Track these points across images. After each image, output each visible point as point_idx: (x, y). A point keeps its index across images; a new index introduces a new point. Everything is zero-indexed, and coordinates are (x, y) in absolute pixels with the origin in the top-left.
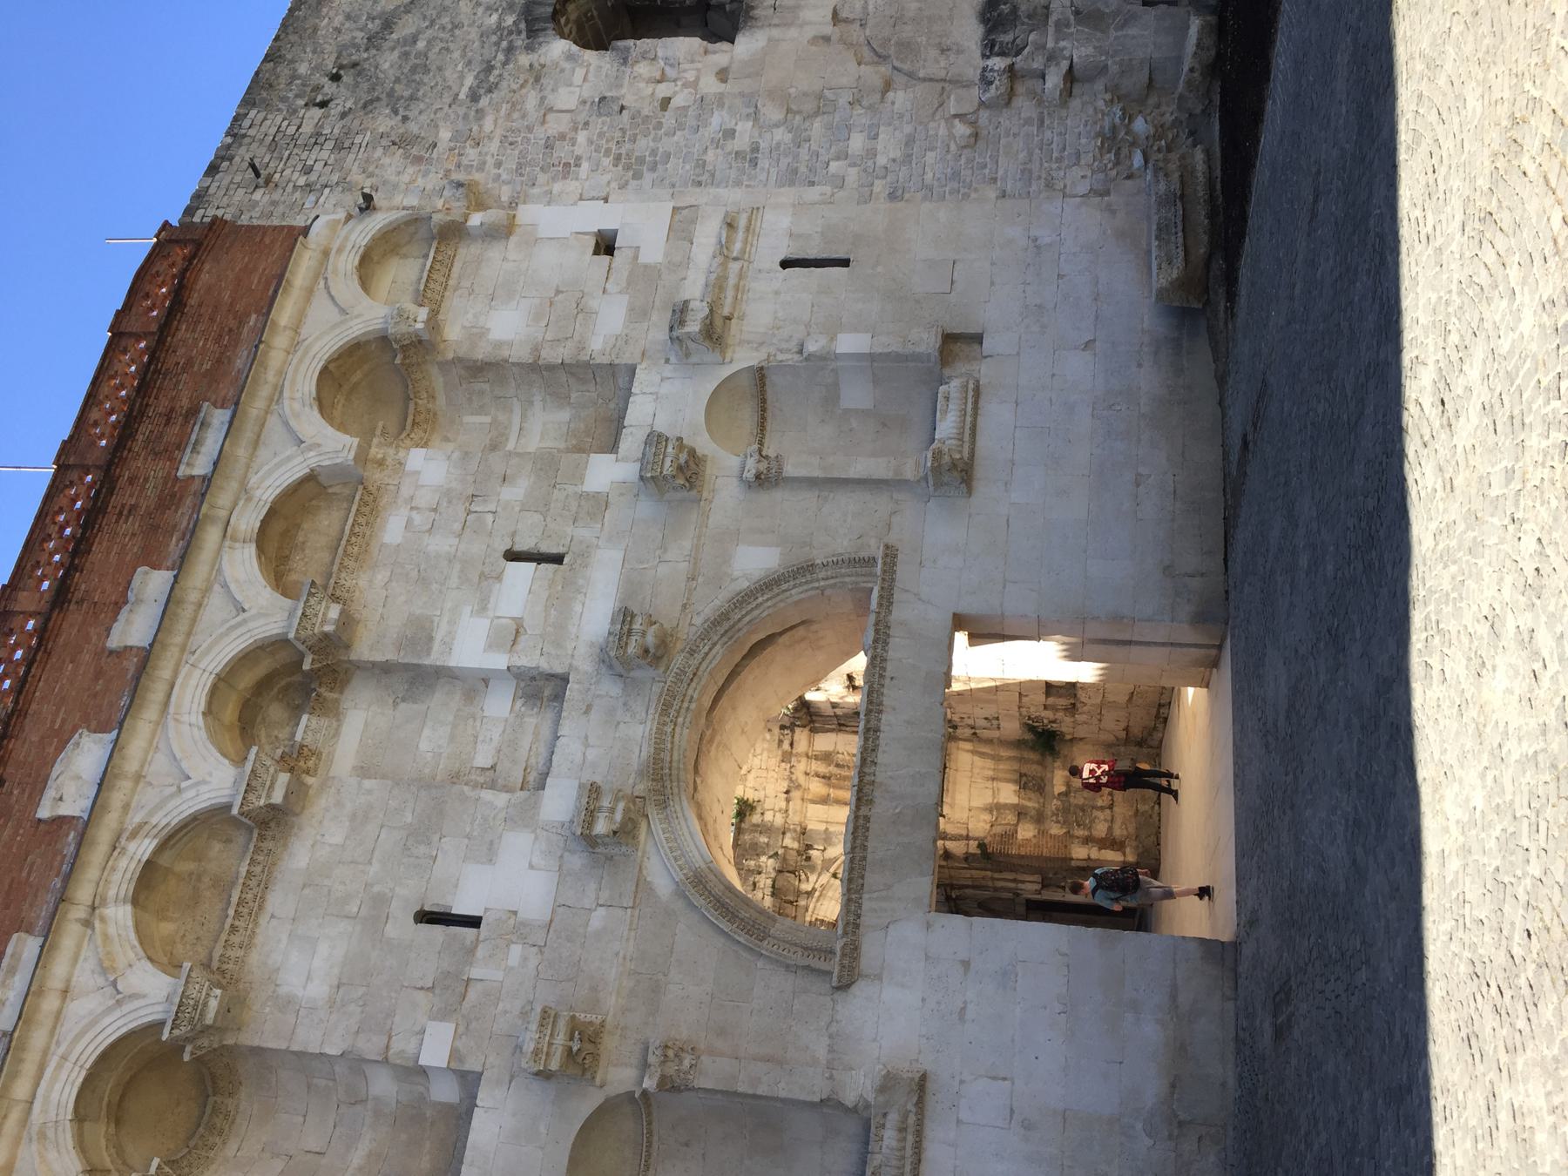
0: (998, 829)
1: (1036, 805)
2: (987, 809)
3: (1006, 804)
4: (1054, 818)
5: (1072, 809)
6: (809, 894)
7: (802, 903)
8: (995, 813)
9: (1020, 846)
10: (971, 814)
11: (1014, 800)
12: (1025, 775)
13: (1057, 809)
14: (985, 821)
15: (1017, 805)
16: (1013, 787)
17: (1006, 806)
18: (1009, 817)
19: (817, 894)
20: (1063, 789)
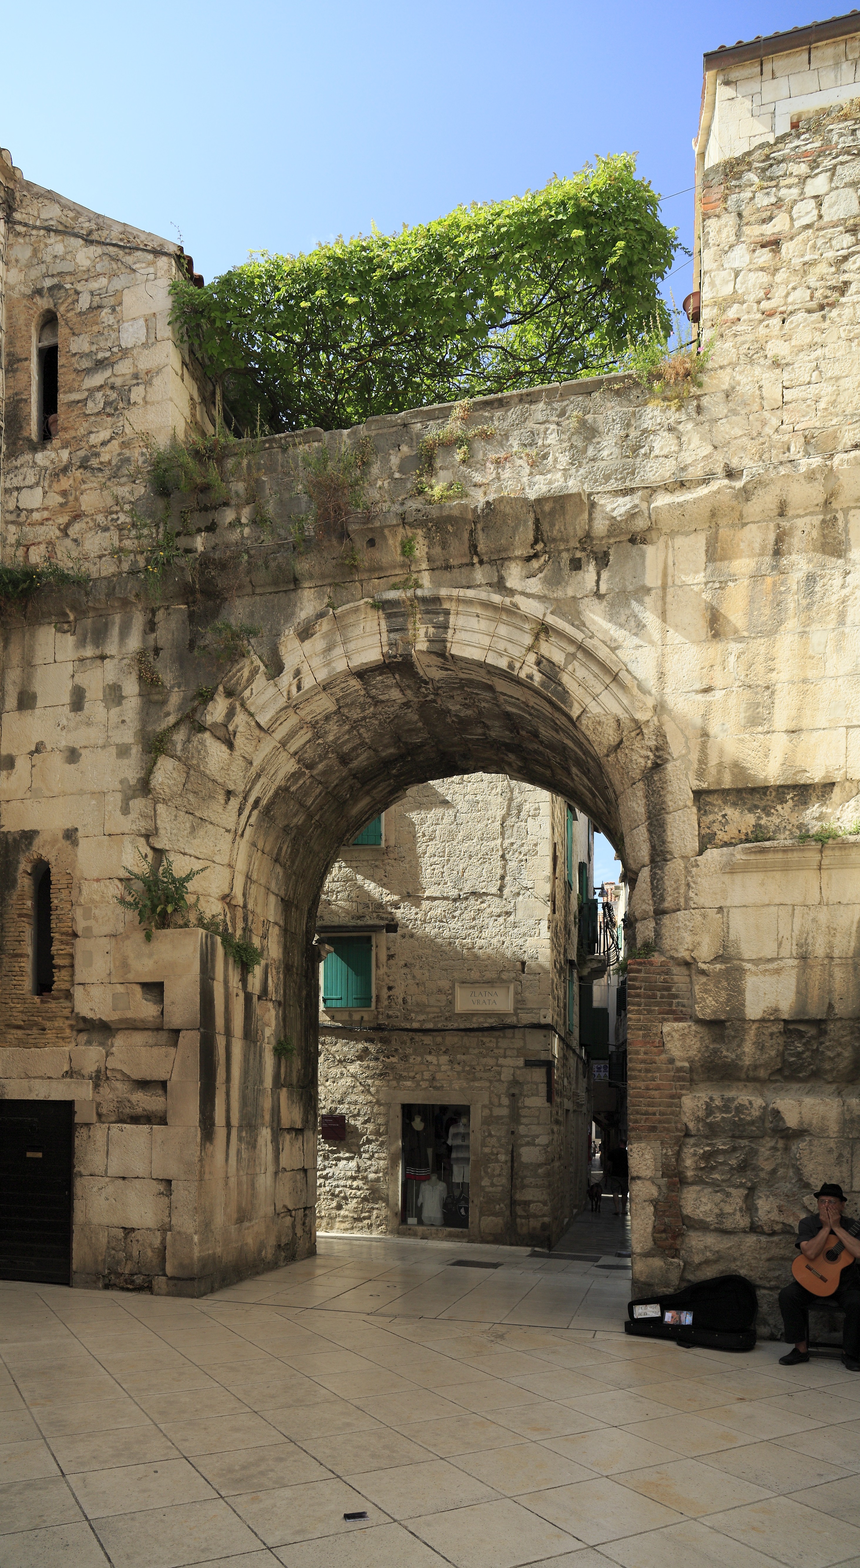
0: (679, 976)
1: (747, 1061)
2: (725, 947)
3: (741, 992)
4: (718, 1102)
5: (744, 1142)
6: (500, 585)
7: (479, 575)
8: (718, 966)
9: (646, 1028)
10: (712, 913)
11: (754, 1009)
12: (823, 1033)
13: (740, 1109)
14: (696, 946)
15: (743, 1020)
16: (786, 1004)
17: (736, 992)
18: (710, 1001)
19: (496, 598)
20: (791, 1121)
